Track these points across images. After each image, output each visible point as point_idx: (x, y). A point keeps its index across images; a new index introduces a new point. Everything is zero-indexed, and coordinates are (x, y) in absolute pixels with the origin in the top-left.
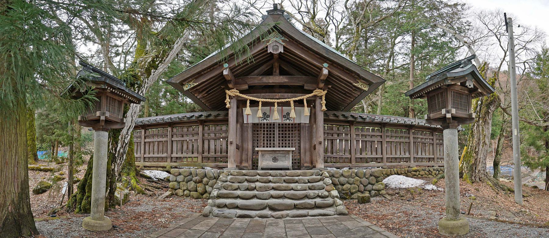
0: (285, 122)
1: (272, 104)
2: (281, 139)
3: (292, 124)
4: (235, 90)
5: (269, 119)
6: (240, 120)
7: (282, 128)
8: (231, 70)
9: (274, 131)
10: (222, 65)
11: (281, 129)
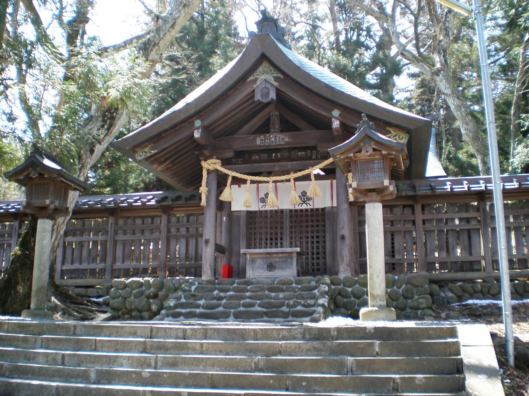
8: (205, 129)
10: (193, 124)
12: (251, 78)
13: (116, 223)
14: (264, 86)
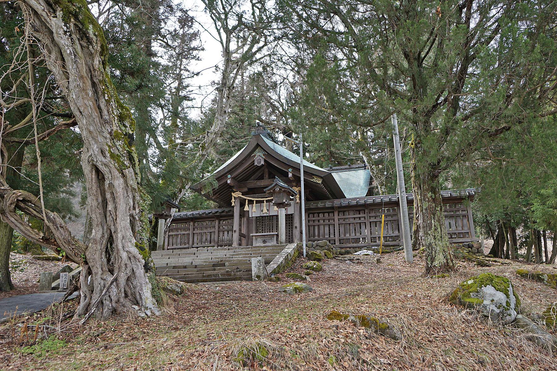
1: (263, 202)
8: (233, 178)
10: (227, 176)
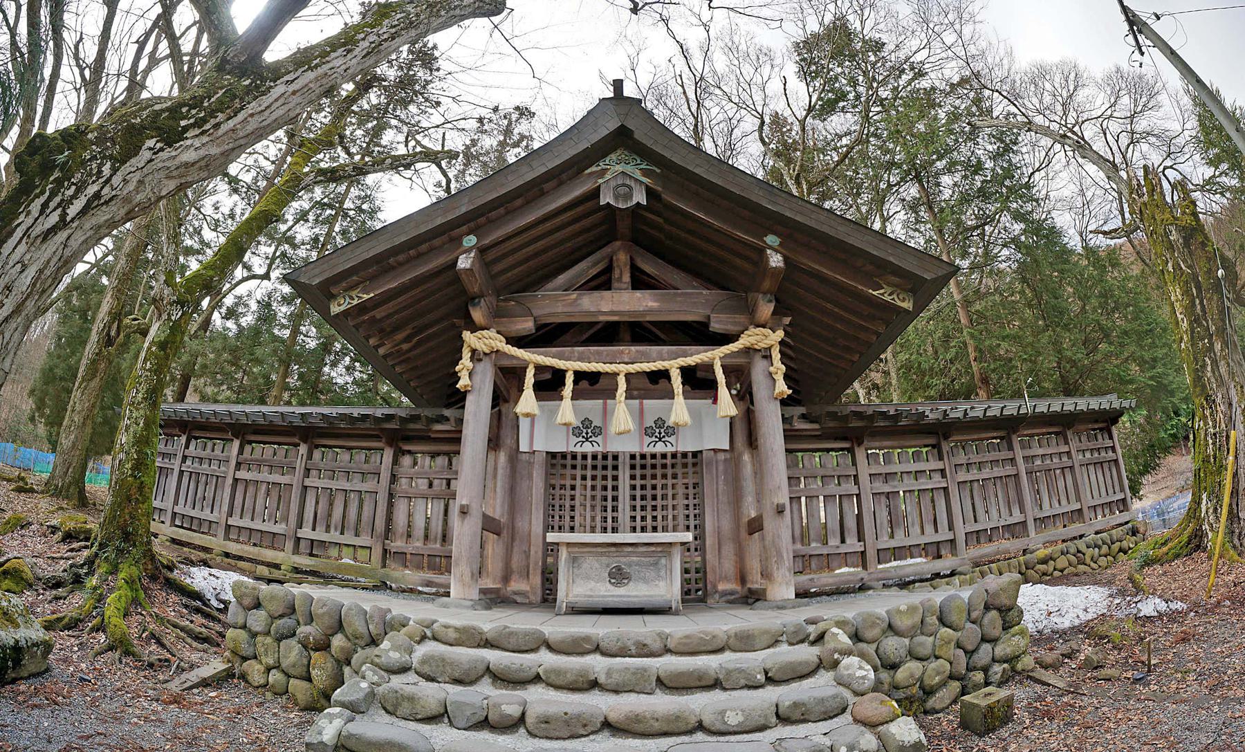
0: (652, 450)
2: (639, 503)
3: (674, 456)
4: (492, 333)
5: (599, 439)
6: (508, 441)
7: (643, 467)
9: (615, 478)
11: (638, 472)
12: (594, 169)
13: (310, 456)
14: (620, 182)
